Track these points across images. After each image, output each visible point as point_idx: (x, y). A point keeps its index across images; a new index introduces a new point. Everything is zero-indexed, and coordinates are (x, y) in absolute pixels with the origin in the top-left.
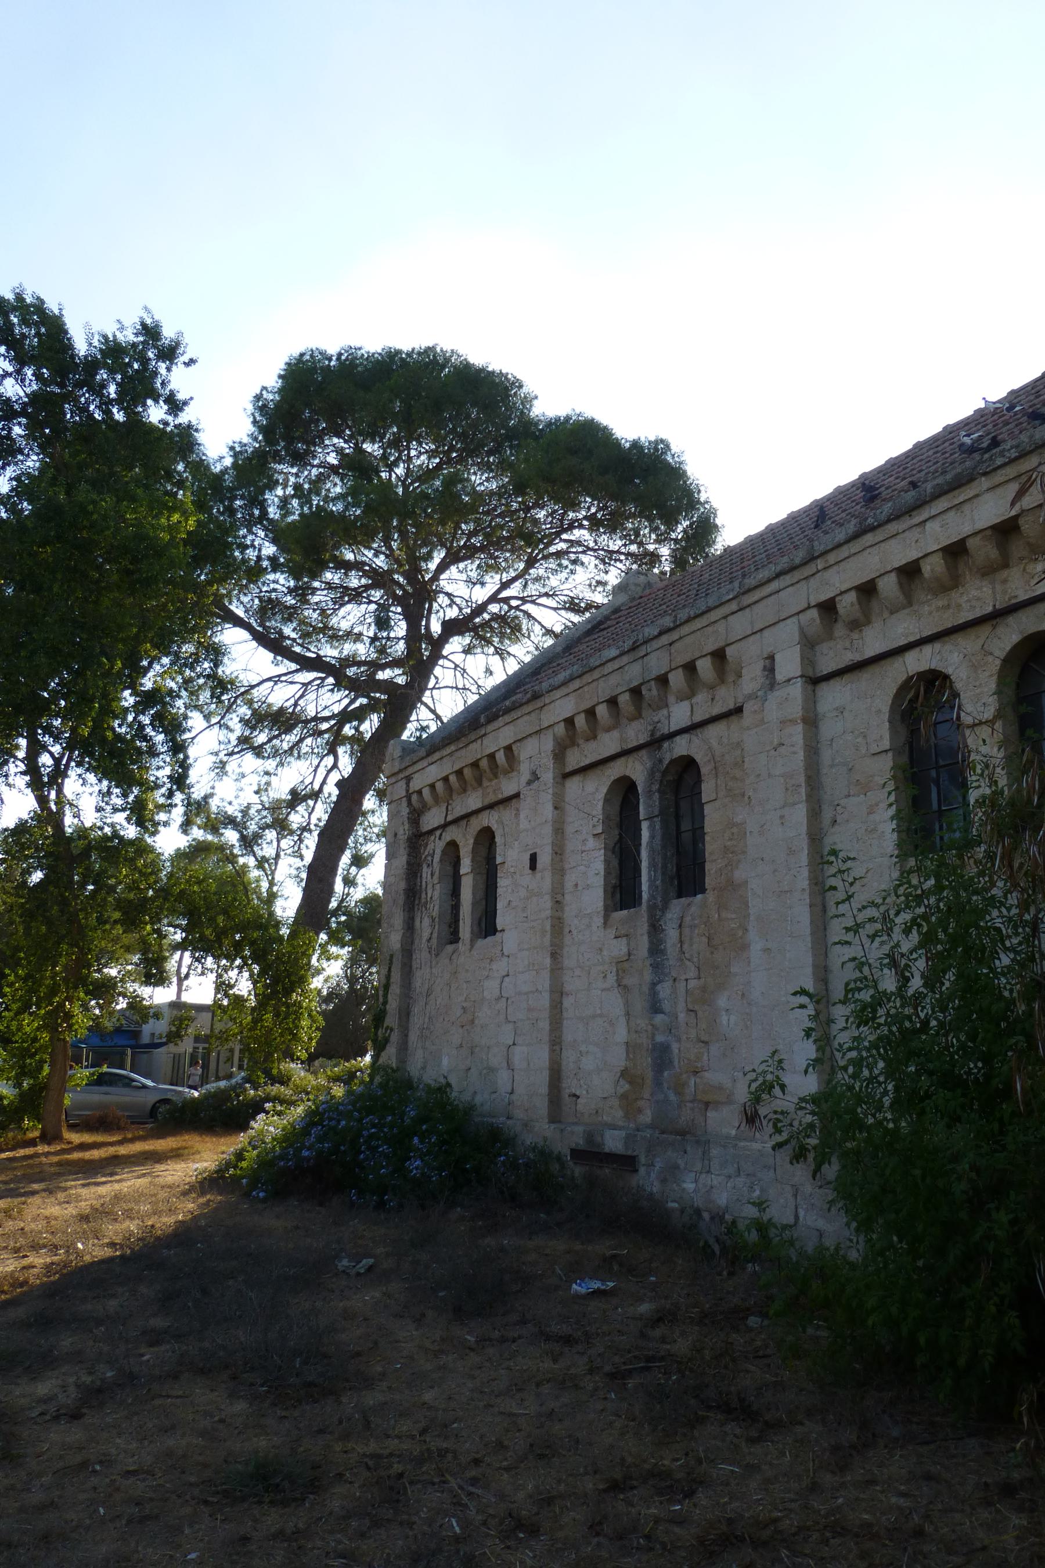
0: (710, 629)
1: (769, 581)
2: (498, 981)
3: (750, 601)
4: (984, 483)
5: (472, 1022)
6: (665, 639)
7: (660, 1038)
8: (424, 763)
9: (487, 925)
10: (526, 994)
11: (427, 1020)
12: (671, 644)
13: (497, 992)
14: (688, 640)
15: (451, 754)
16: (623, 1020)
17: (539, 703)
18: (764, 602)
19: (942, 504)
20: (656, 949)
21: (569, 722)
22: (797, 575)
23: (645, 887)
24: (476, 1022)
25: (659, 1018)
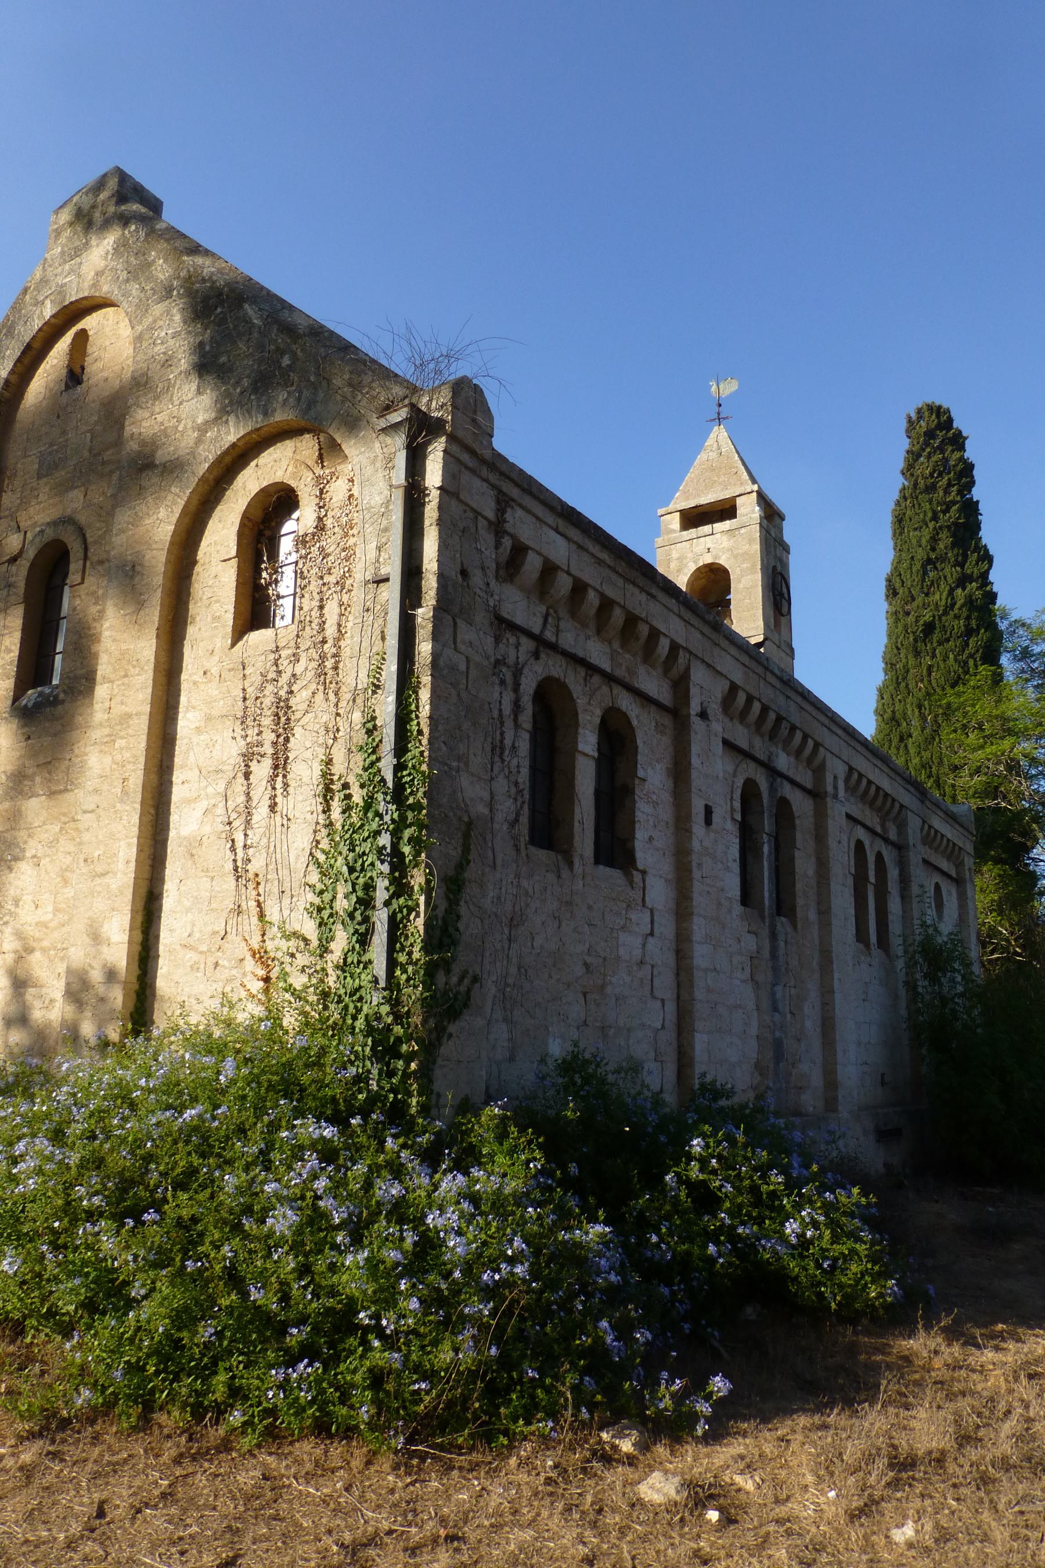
2: (639, 941)
4: (886, 769)
5: (603, 987)
6: (799, 699)
7: (777, 1034)
8: (550, 519)
9: (615, 850)
10: (706, 970)
11: (513, 970)
13: (638, 953)
15: (600, 562)
16: (755, 1013)
17: (714, 636)
19: (879, 763)
20: (774, 955)
21: (734, 688)
22: (847, 738)
23: (766, 894)
24: (609, 990)
25: (777, 1017)
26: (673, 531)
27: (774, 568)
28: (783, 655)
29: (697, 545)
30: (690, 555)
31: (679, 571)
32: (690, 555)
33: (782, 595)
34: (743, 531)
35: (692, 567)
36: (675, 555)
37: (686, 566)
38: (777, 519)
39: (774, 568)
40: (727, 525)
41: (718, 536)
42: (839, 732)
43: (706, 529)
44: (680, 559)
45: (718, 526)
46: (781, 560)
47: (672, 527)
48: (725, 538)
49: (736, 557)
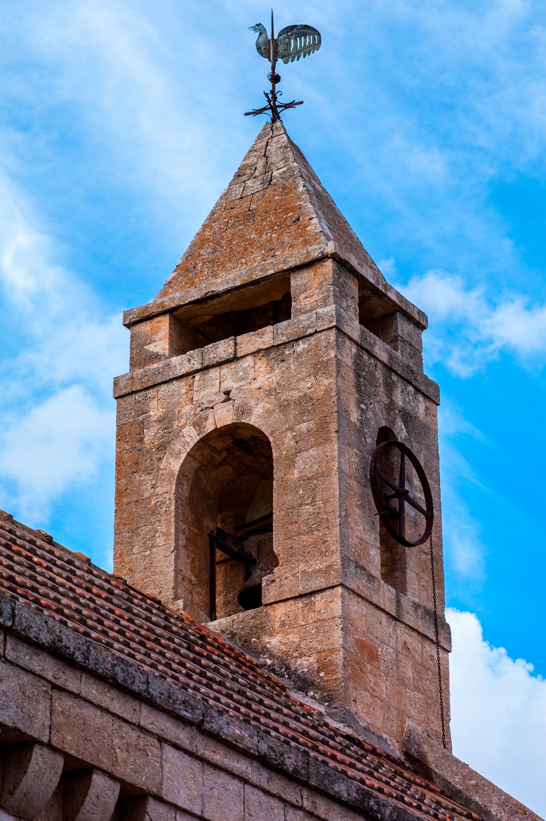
0: (134, 735)
1: (244, 753)
3: (209, 754)
6: (48, 667)
12: (54, 687)
14: (88, 712)
18: (223, 779)
22: (277, 786)
26: (156, 357)
27: (385, 434)
28: (413, 641)
29: (203, 387)
30: (187, 409)
31: (163, 447)
32: (187, 409)
33: (403, 495)
34: (301, 346)
35: (191, 437)
36: (155, 410)
37: (178, 434)
38: (403, 327)
39: (385, 434)
40: (266, 336)
41: (249, 362)
42: (241, 766)
43: (223, 348)
44: (166, 420)
45: (249, 342)
46: (408, 417)
47: (152, 348)
48: (262, 365)
49: (284, 407)
